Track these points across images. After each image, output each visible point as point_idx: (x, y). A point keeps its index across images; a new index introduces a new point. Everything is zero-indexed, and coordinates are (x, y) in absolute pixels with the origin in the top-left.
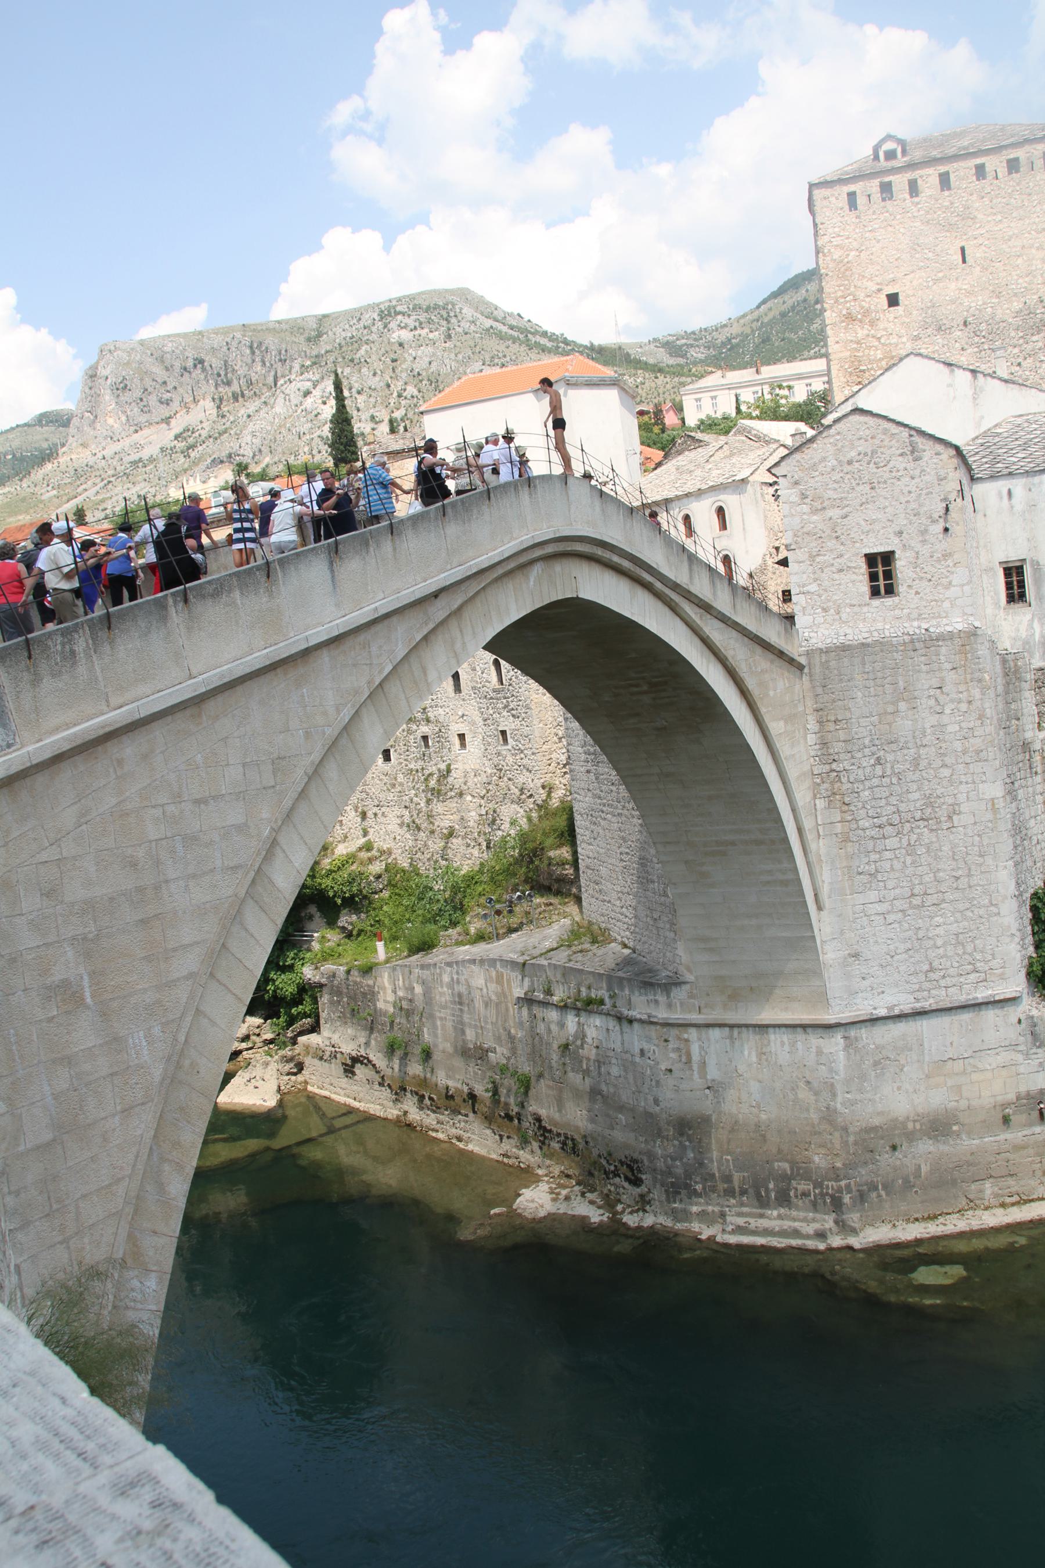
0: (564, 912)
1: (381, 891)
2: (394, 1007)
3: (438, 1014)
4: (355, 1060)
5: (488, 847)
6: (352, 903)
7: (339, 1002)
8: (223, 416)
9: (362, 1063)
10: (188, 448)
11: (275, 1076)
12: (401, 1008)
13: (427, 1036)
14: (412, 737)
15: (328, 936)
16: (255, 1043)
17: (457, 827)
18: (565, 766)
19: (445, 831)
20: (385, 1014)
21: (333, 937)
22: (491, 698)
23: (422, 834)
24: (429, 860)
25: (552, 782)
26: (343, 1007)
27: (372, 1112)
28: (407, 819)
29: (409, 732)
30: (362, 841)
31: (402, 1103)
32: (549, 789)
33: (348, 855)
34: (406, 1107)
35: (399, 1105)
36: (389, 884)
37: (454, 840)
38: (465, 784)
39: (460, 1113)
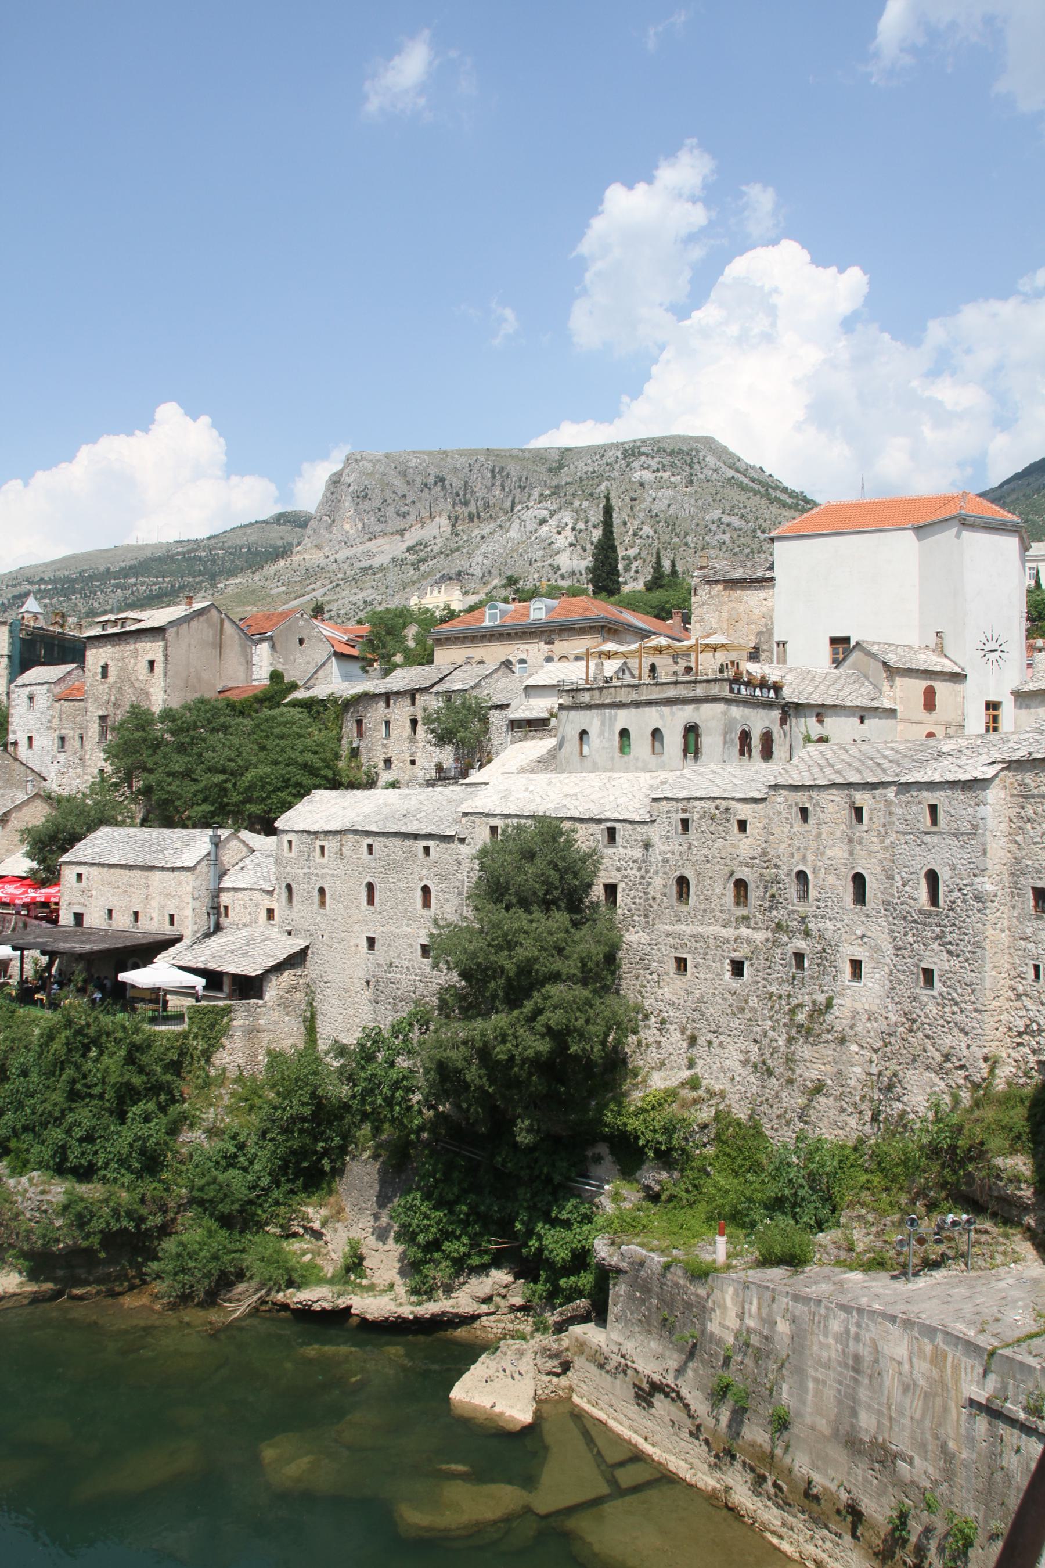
0: (1014, 1251)
1: (704, 1146)
2: (736, 1338)
3: (811, 1372)
4: (656, 1388)
5: (874, 1119)
6: (665, 1158)
7: (643, 1301)
8: (457, 535)
9: (667, 1395)
10: (419, 562)
11: (531, 1375)
12: (748, 1345)
13: (786, 1395)
14: (779, 951)
15: (624, 1192)
16: (498, 1307)
17: (829, 1082)
18: (1020, 1034)
19: (810, 1084)
20: (719, 1342)
21: (631, 1195)
22: (915, 921)
23: (774, 1081)
24: (778, 1117)
25: (998, 1053)
26: (648, 1309)
27: (672, 1468)
28: (754, 1057)
29: (776, 943)
30: (686, 1074)
31: (724, 1473)
32: (993, 1062)
33: (666, 1091)
34: (730, 1482)
35: (718, 1475)
36: (718, 1138)
37: (822, 1099)
38: (851, 1028)
39: (826, 1527)
